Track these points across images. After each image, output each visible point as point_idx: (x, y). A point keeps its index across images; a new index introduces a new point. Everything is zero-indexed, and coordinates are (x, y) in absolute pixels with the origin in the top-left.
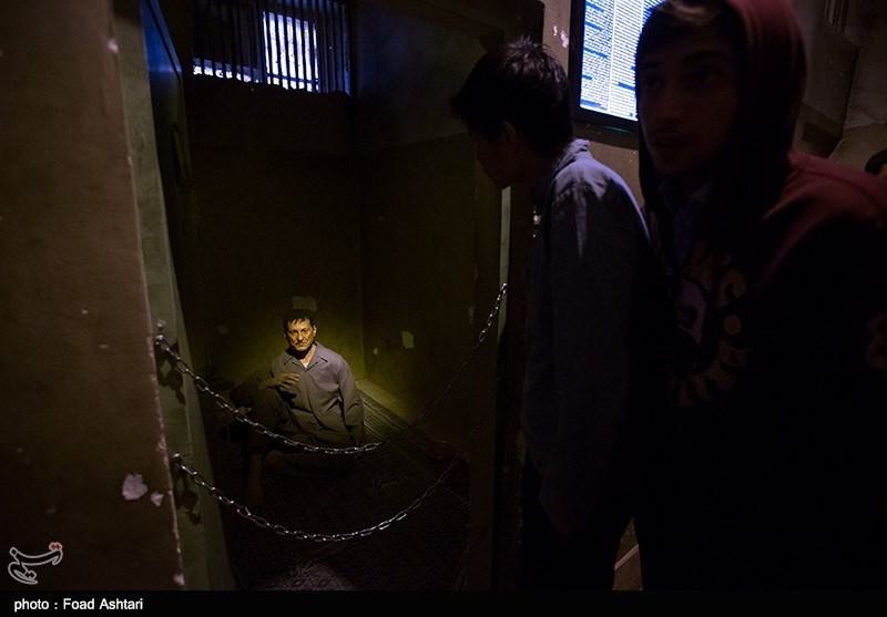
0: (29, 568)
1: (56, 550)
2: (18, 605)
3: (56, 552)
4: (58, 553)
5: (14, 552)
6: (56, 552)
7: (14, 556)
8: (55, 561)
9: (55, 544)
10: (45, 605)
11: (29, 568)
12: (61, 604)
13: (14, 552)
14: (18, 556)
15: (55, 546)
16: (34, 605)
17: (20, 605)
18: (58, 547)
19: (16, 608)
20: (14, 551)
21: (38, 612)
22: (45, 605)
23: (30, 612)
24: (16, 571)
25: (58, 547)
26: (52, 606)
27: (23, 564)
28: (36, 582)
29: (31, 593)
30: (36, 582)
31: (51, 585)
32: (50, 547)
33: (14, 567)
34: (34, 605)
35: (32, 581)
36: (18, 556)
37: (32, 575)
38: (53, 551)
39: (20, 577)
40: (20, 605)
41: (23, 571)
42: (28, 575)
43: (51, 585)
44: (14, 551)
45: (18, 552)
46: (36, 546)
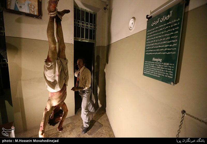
0: (7, 133)
2: (3, 141)
5: (3, 129)
7: (3, 130)
10: (11, 141)
11: (7, 133)
13: (3, 129)
14: (4, 130)
19: (3, 142)
20: (3, 129)
21: (9, 143)
22: (11, 141)
23: (6, 143)
24: (4, 133)
27: (6, 132)
32: (12, 128)
33: (3, 132)
36: (4, 130)
37: (7, 134)
39: (5, 135)
41: (5, 133)
42: (6, 134)
44: (3, 129)
45: (4, 129)
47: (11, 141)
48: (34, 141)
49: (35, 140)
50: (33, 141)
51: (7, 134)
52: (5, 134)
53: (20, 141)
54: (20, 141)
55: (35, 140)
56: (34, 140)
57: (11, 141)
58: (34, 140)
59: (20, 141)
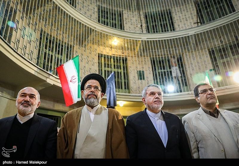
0: (8, 153)
1: (15, 148)
3: (15, 149)
4: (15, 149)
5: (3, 148)
6: (15, 149)
7: (4, 150)
8: (15, 151)
9: (15, 146)
10: (11, 163)
11: (8, 153)
12: (15, 162)
13: (3, 148)
14: (5, 150)
15: (15, 147)
16: (8, 163)
17: (4, 163)
18: (15, 147)
19: (3, 163)
20: (3, 148)
22: (11, 163)
24: (4, 154)
25: (15, 147)
26: (13, 163)
28: (9, 157)
29: (7, 159)
30: (9, 157)
31: (14, 157)
32: (13, 147)
33: (3, 153)
34: (8, 163)
35: (8, 156)
36: (5, 150)
37: (8, 155)
38: (14, 148)
40: (4, 163)
41: (6, 154)
42: (7, 155)
43: (14, 157)
44: (3, 148)
46: (9, 147)
47: (10, 162)
48: (31, 162)
49: (32, 161)
50: (29, 162)
51: (8, 154)
52: (6, 155)
53: (17, 163)
54: (16, 162)
55: (32, 161)
56: (31, 161)
57: (10, 162)
58: (31, 161)
59: (17, 163)
